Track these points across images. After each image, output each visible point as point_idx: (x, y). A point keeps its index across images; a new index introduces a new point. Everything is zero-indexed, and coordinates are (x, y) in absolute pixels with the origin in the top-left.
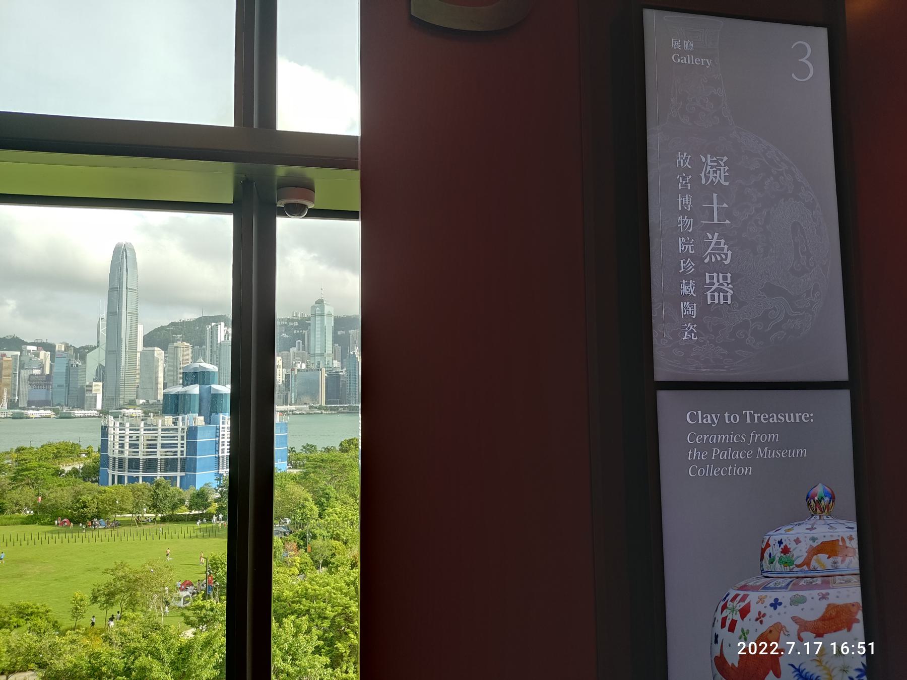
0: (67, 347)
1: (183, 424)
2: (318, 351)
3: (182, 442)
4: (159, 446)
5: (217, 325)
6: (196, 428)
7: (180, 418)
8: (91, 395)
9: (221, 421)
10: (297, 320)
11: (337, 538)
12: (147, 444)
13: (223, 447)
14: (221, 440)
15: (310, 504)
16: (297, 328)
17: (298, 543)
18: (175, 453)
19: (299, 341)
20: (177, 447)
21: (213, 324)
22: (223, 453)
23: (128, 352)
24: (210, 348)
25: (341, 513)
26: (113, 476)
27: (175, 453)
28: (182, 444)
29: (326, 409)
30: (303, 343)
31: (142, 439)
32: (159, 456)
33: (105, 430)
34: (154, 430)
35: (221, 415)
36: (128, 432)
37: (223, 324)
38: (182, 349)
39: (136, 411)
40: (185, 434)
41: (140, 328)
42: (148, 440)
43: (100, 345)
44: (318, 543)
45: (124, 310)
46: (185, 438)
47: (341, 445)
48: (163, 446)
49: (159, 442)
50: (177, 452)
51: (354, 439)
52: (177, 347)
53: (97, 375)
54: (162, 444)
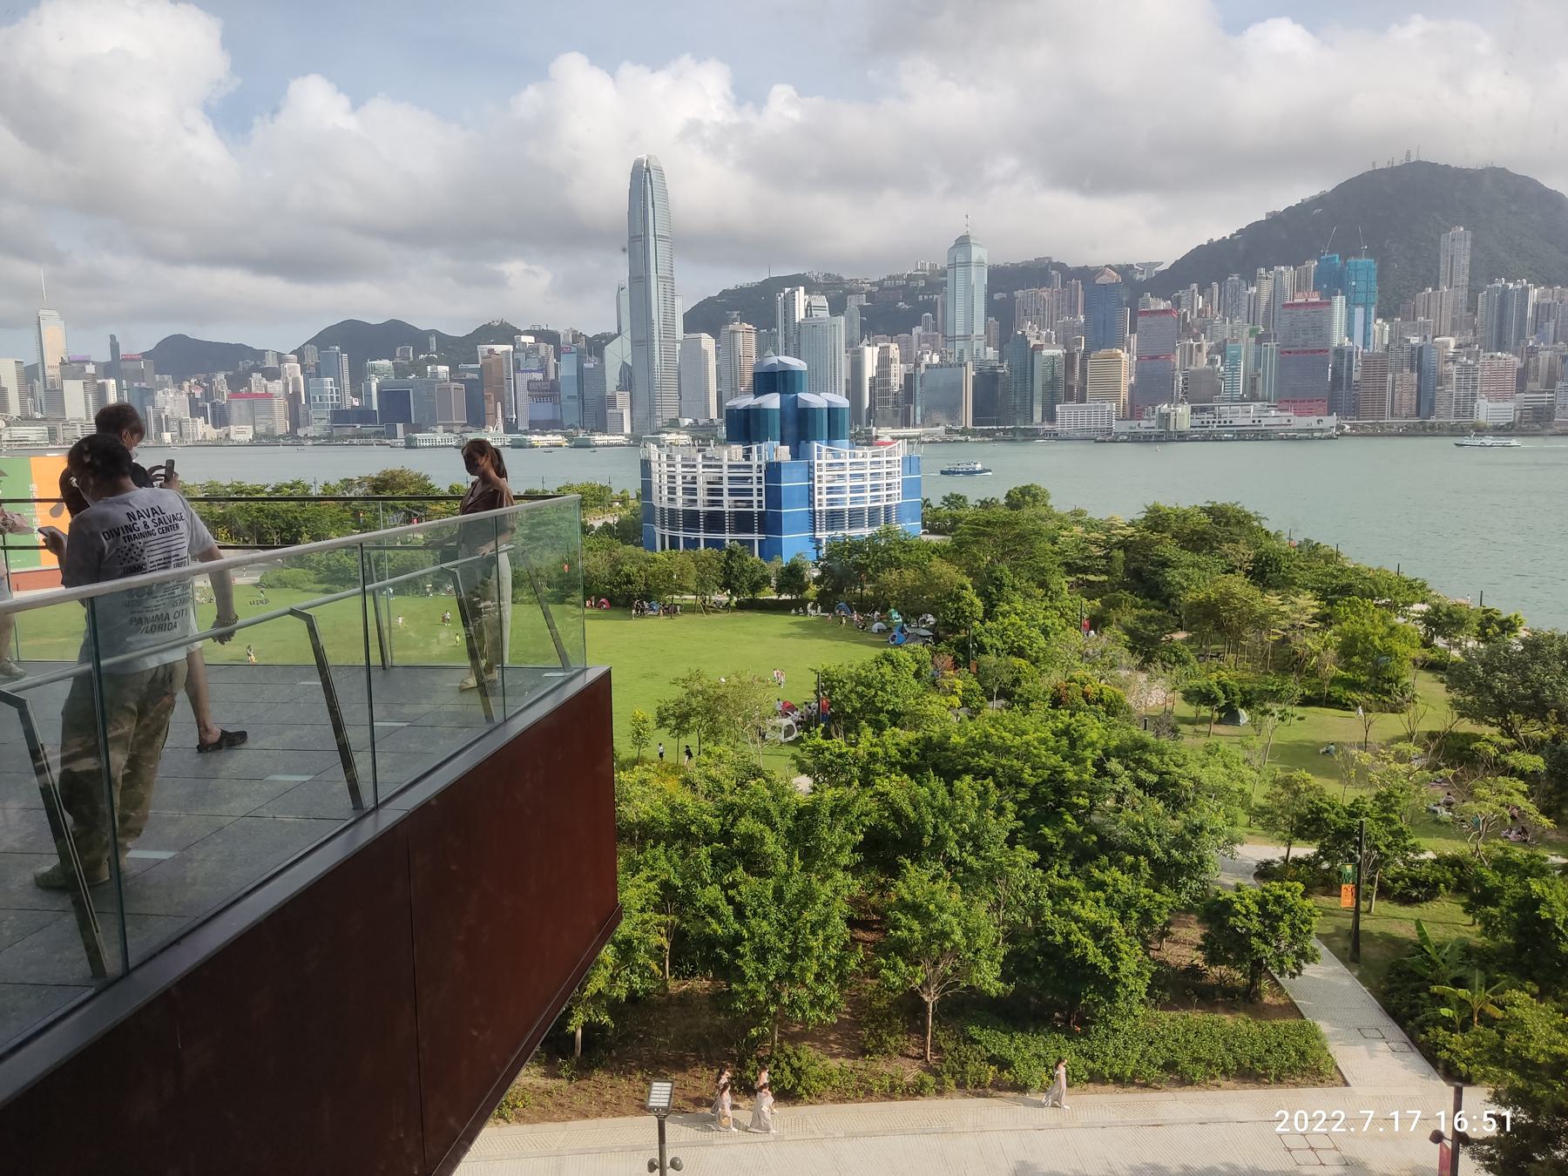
0: (577, 337)
2: (960, 332)
3: (760, 487)
4: (726, 492)
6: (779, 464)
7: (754, 448)
8: (615, 411)
9: (816, 453)
11: (1020, 653)
12: (709, 489)
13: (820, 497)
14: (817, 485)
15: (970, 595)
16: (923, 291)
17: (955, 657)
19: (928, 314)
20: (752, 495)
21: (787, 290)
22: (820, 505)
25: (1024, 613)
26: (663, 536)
29: (974, 433)
31: (700, 480)
32: (726, 509)
33: (646, 465)
34: (716, 466)
35: (816, 444)
36: (679, 469)
37: (802, 289)
39: (681, 437)
40: (763, 475)
41: (678, 302)
42: (709, 483)
43: (623, 330)
44: (990, 659)
45: (653, 274)
46: (763, 480)
47: (1008, 496)
48: (732, 492)
49: (726, 486)
50: (752, 501)
51: (1032, 485)
53: (621, 381)
54: (729, 490)
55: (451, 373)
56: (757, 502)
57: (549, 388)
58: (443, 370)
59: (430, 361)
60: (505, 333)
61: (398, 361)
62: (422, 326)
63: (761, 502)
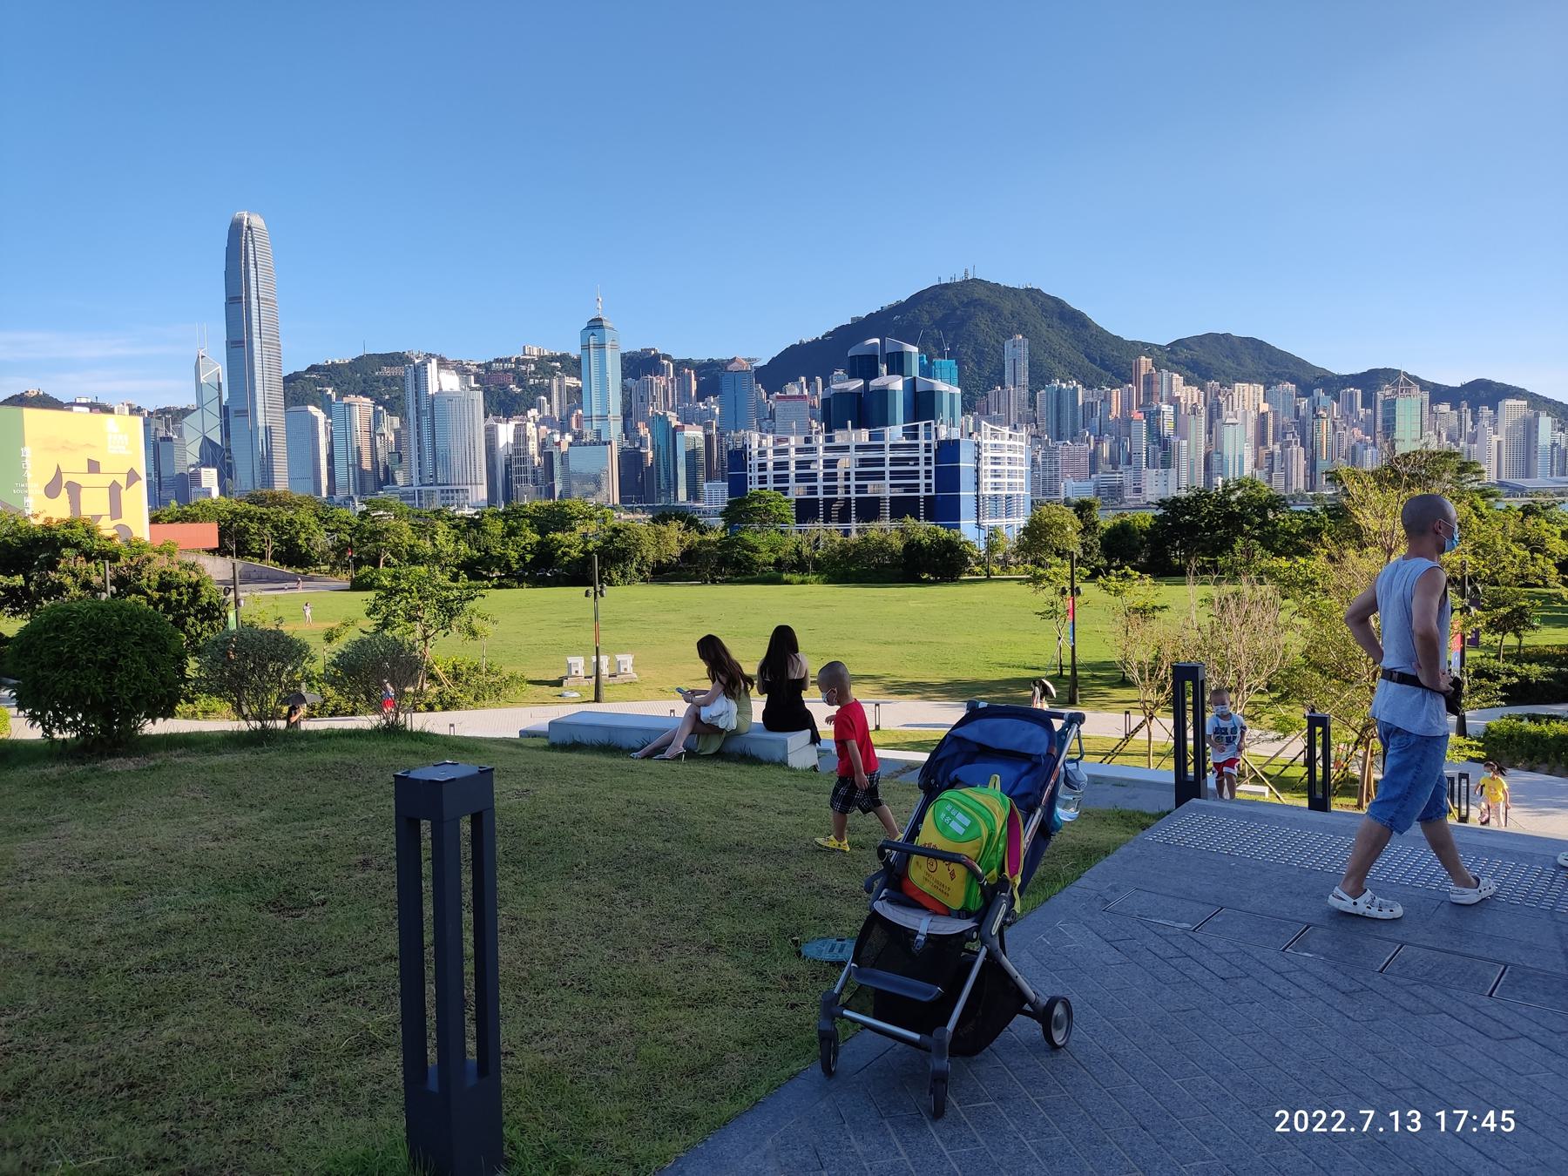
1: (928, 437)
3: (928, 468)
4: (887, 475)
7: (922, 424)
10: (533, 361)
18: (915, 488)
20: (918, 478)
27: (915, 488)
28: (928, 472)
30: (550, 401)
40: (932, 454)
46: (933, 461)
48: (894, 475)
49: (887, 469)
56: (924, 486)
63: (930, 485)
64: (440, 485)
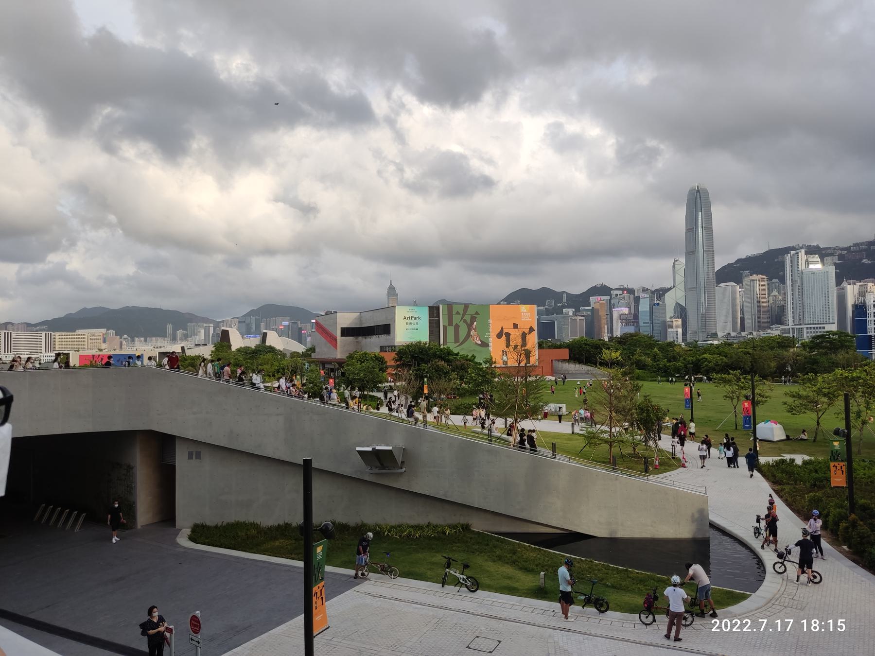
5: (798, 253)
8: (672, 330)
21: (793, 252)
23: (707, 287)
24: (791, 278)
38: (758, 281)
52: (753, 280)
53: (675, 313)
55: (576, 312)
57: (632, 318)
58: (570, 311)
59: (565, 307)
60: (603, 290)
61: (547, 307)
62: (558, 289)
64: (806, 324)
